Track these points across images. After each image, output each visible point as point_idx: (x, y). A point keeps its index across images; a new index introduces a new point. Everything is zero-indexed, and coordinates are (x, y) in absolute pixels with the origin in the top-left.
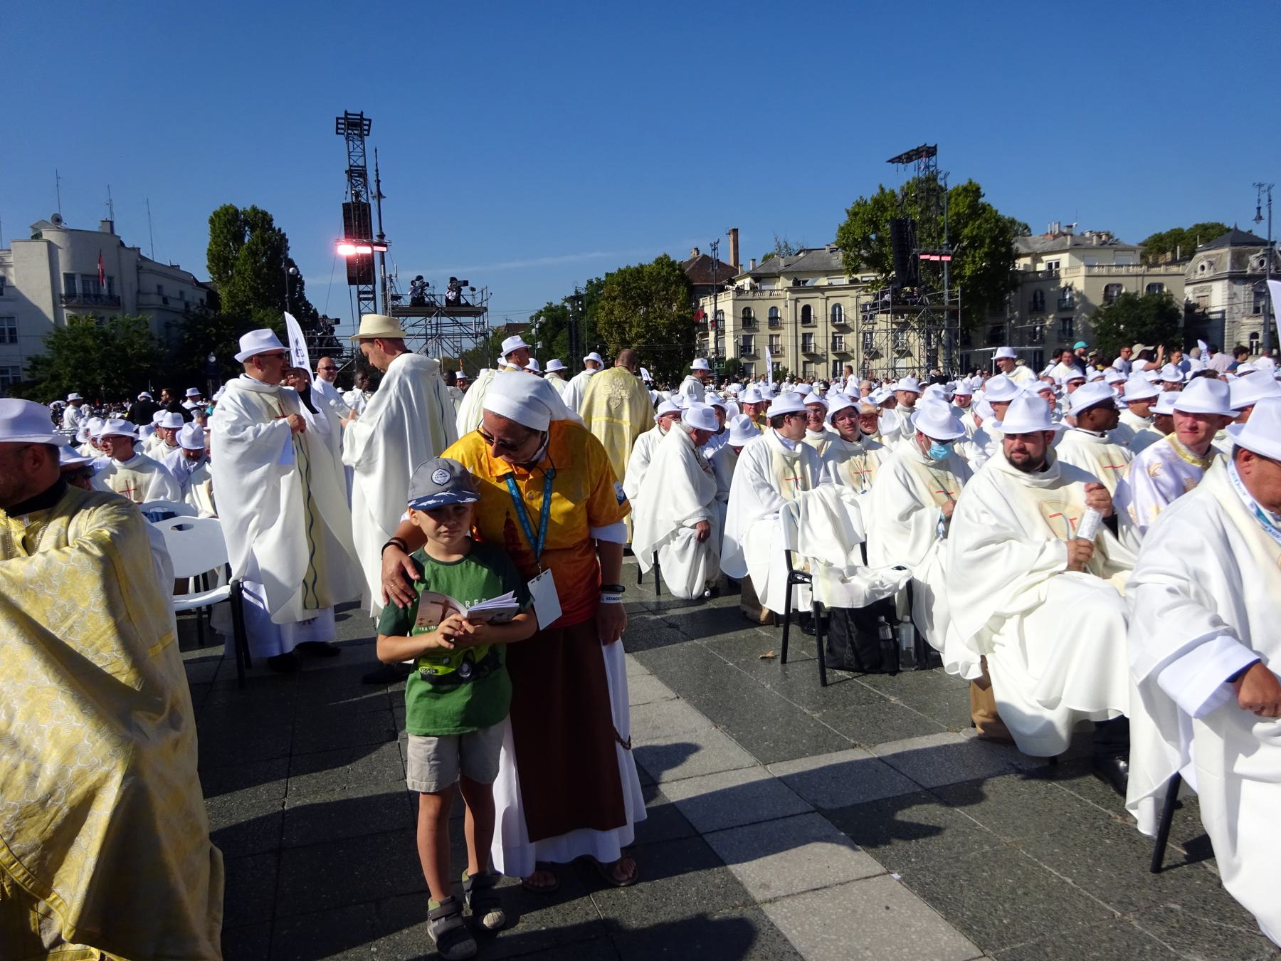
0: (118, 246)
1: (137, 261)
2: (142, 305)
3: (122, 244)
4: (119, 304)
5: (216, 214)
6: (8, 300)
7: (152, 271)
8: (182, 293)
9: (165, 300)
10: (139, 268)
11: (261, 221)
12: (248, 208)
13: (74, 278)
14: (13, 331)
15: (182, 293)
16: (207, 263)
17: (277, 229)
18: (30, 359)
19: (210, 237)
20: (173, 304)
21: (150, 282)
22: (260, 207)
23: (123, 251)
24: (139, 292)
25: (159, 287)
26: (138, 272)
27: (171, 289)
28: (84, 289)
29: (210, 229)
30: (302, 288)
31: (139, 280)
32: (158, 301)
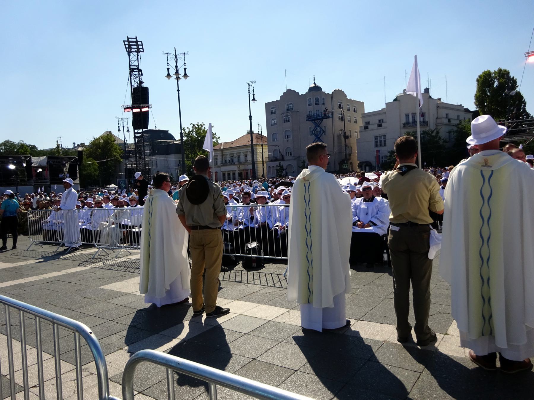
0: (428, 98)
1: (437, 104)
2: (438, 124)
3: (430, 97)
4: (427, 125)
5: (480, 77)
6: (384, 128)
7: (443, 107)
8: (458, 116)
9: (449, 121)
10: (438, 107)
11: (503, 74)
12: (497, 70)
13: (409, 115)
14: (385, 141)
15: (458, 116)
16: (474, 101)
17: (512, 77)
18: (389, 152)
19: (476, 88)
20: (453, 122)
21: (443, 113)
22: (503, 68)
23: (430, 99)
24: (437, 118)
25: (447, 115)
26: (437, 109)
27: (453, 115)
28: (413, 120)
29: (476, 84)
30: (525, 106)
31: (437, 112)
32: (446, 121)
